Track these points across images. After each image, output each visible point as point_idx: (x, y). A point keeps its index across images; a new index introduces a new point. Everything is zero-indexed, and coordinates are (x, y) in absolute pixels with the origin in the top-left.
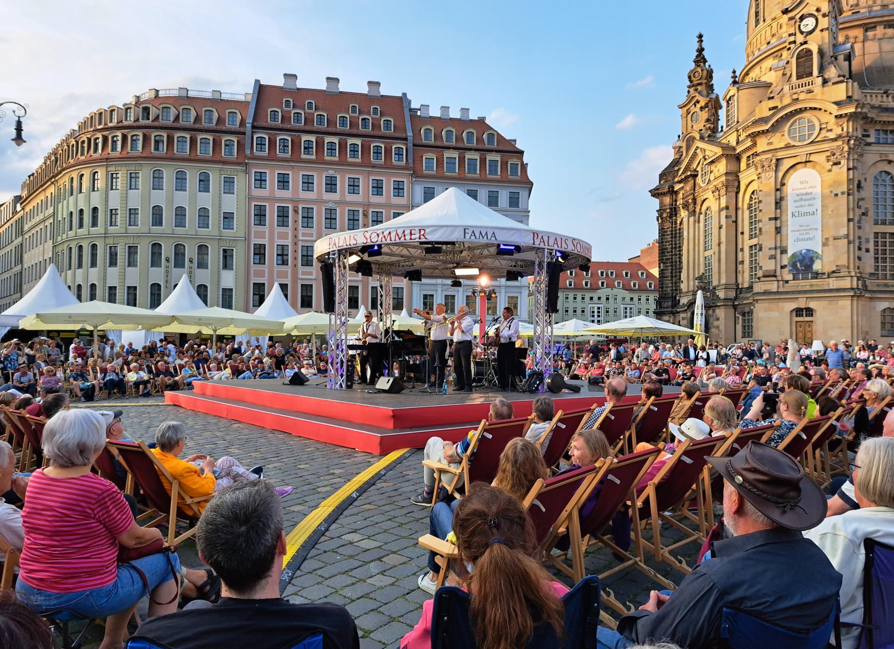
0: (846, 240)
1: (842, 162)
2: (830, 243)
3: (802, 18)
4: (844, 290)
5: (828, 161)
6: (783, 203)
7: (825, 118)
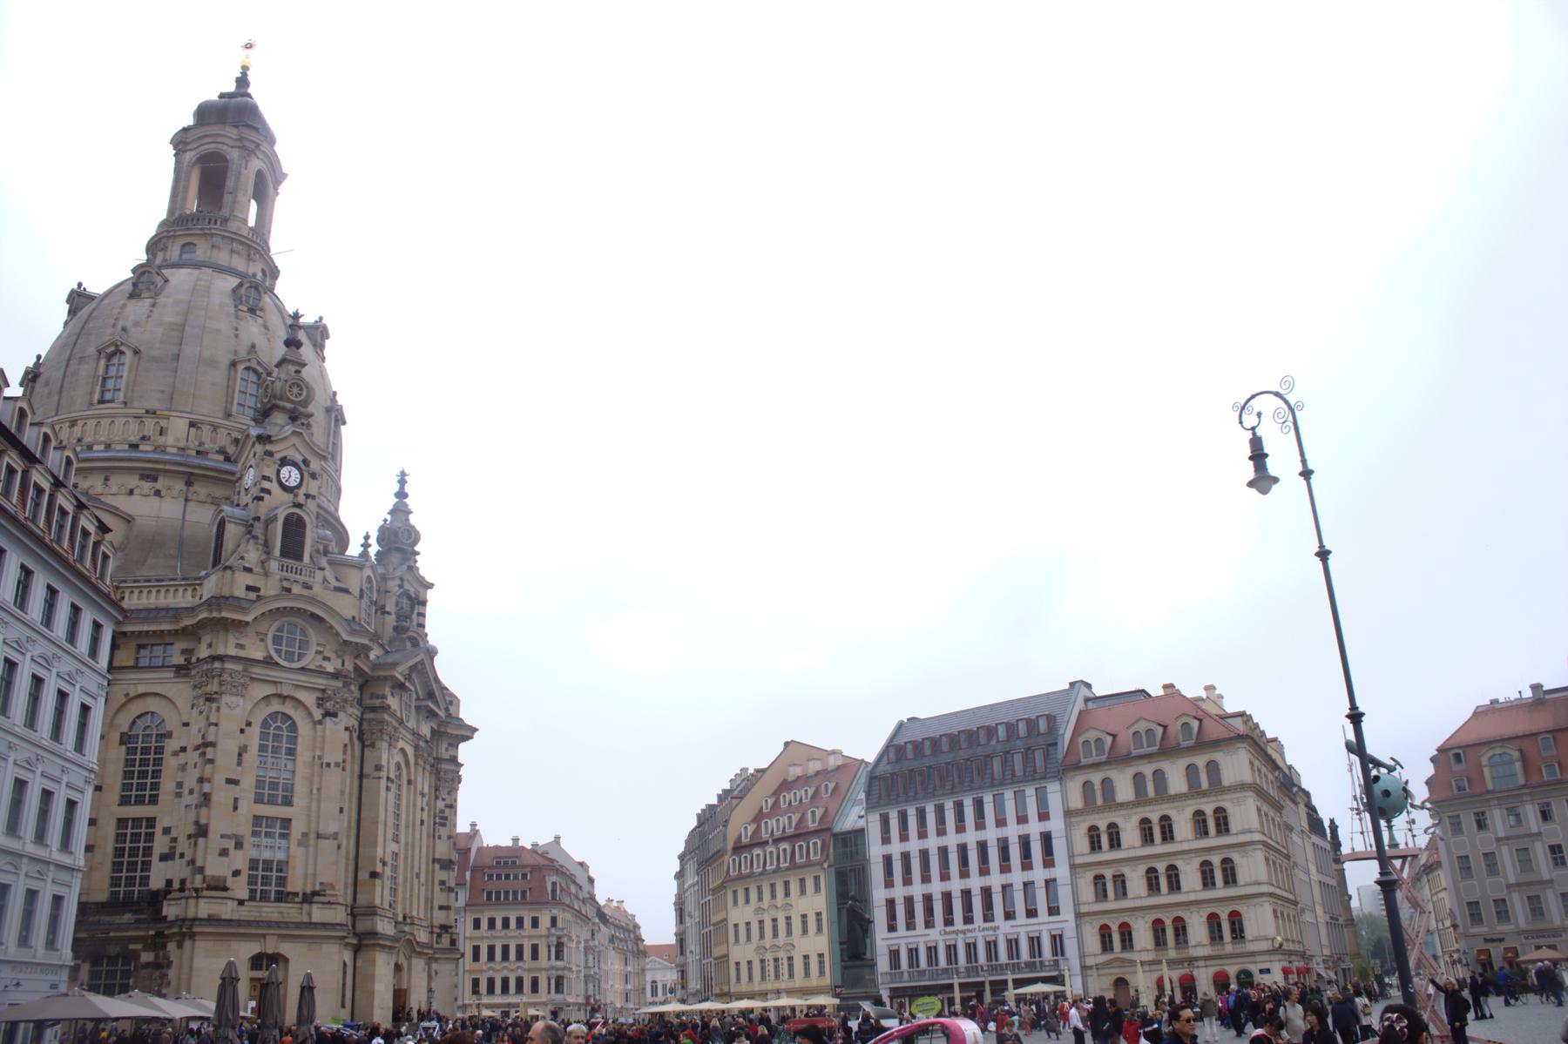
0: (335, 843)
1: (341, 715)
2: (312, 842)
3: (284, 462)
4: (333, 926)
5: (319, 706)
6: (245, 756)
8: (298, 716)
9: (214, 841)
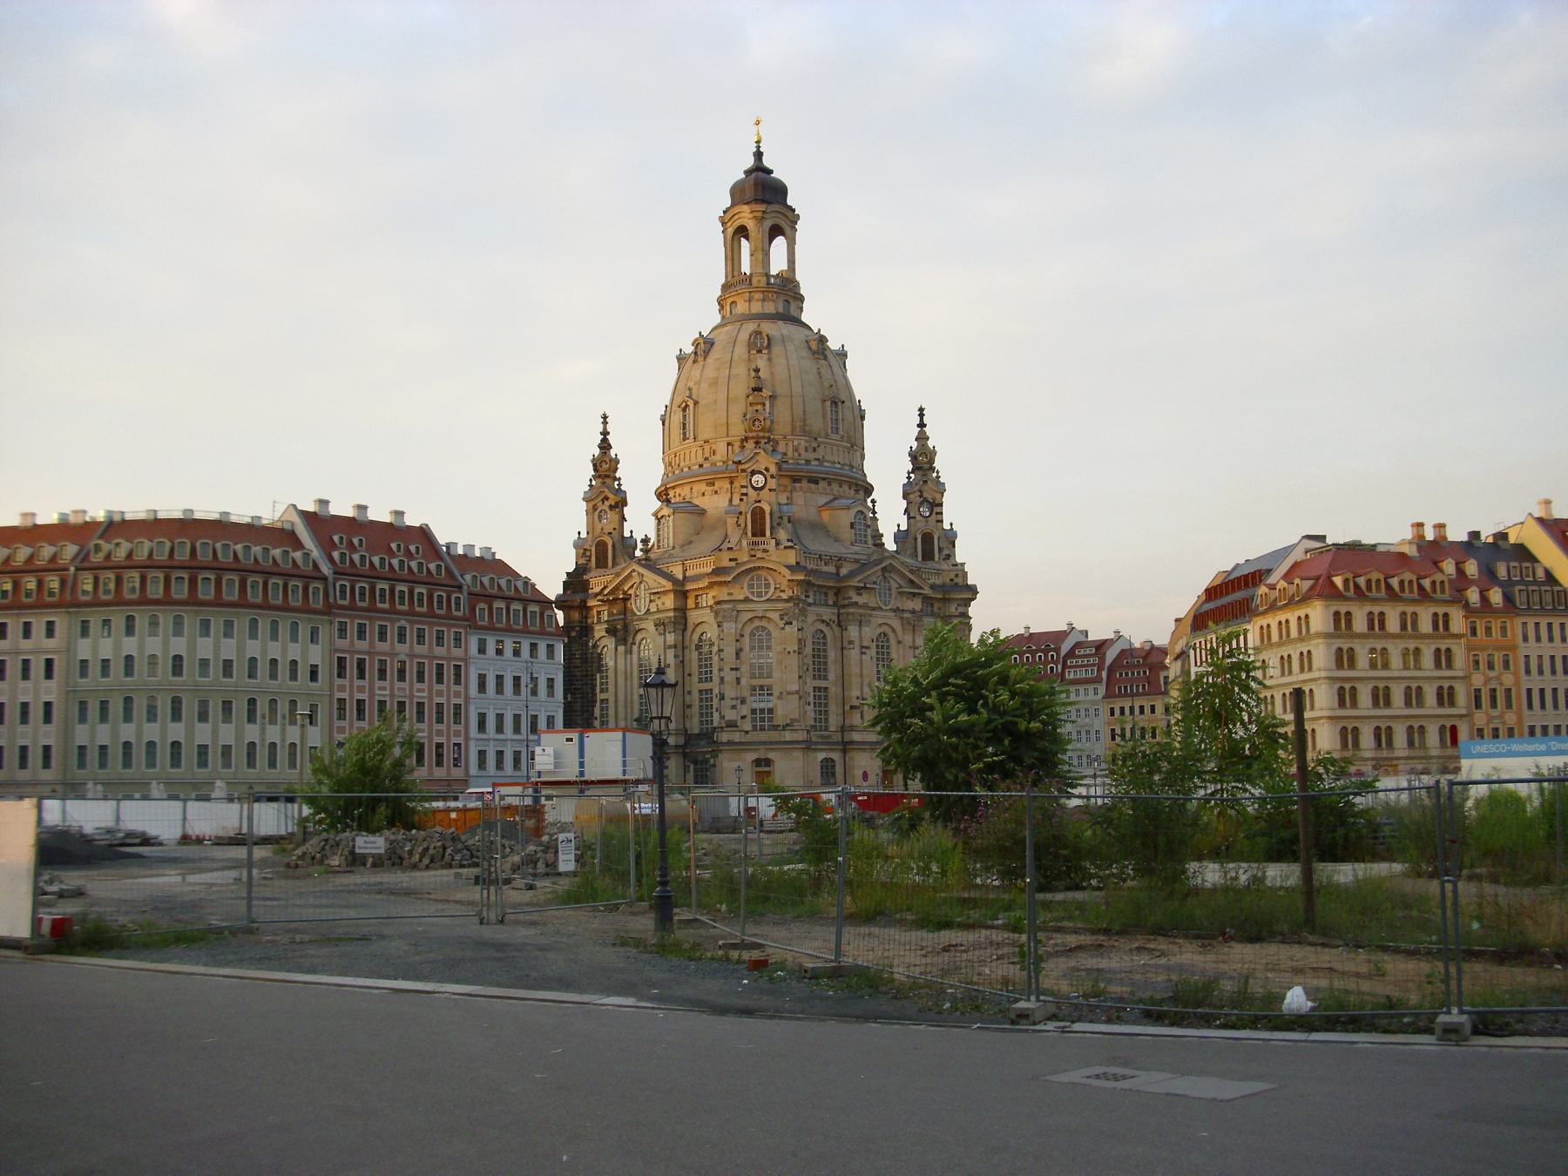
3: (753, 473)
4: (797, 742)
7: (779, 579)
8: (770, 627)
9: (728, 702)
